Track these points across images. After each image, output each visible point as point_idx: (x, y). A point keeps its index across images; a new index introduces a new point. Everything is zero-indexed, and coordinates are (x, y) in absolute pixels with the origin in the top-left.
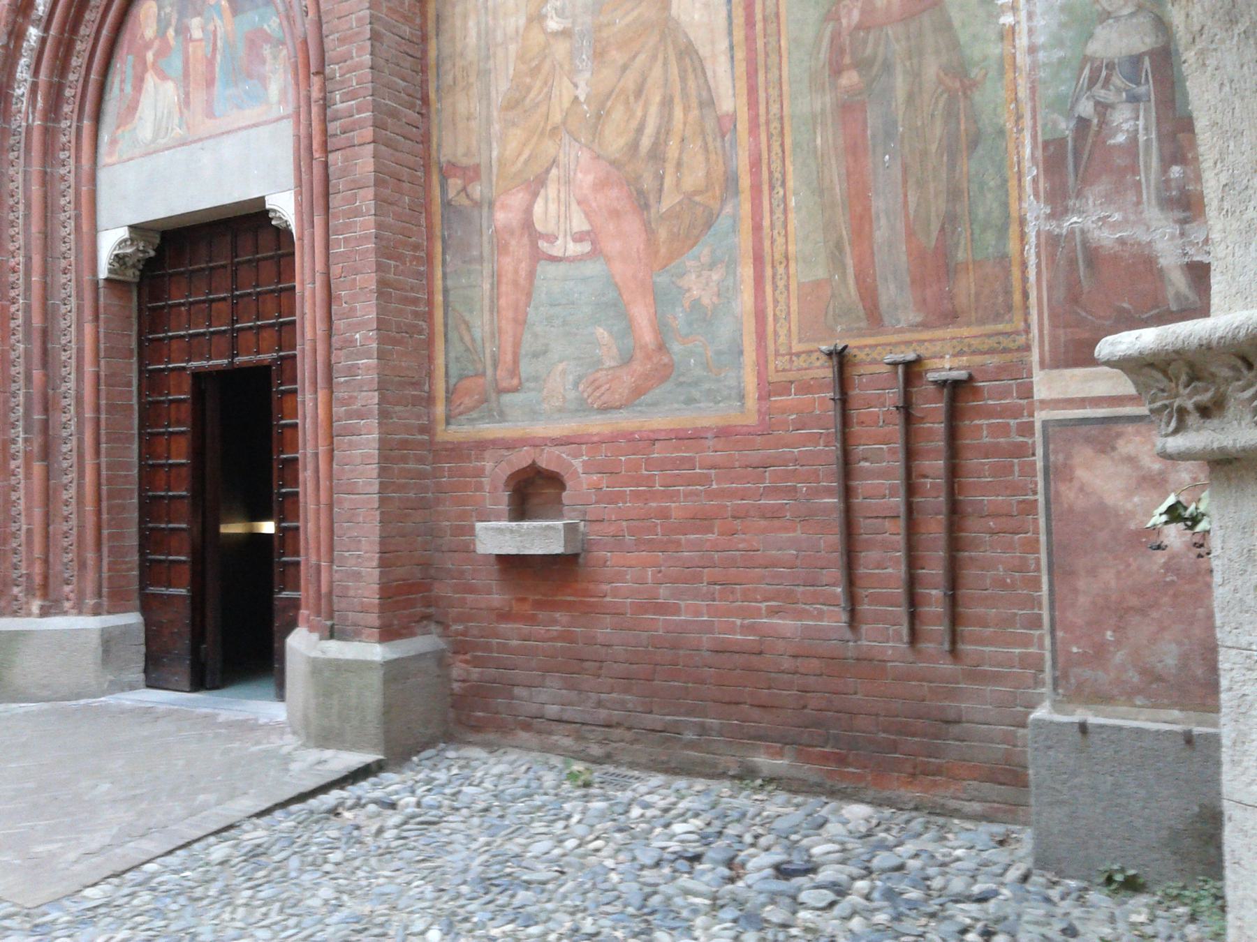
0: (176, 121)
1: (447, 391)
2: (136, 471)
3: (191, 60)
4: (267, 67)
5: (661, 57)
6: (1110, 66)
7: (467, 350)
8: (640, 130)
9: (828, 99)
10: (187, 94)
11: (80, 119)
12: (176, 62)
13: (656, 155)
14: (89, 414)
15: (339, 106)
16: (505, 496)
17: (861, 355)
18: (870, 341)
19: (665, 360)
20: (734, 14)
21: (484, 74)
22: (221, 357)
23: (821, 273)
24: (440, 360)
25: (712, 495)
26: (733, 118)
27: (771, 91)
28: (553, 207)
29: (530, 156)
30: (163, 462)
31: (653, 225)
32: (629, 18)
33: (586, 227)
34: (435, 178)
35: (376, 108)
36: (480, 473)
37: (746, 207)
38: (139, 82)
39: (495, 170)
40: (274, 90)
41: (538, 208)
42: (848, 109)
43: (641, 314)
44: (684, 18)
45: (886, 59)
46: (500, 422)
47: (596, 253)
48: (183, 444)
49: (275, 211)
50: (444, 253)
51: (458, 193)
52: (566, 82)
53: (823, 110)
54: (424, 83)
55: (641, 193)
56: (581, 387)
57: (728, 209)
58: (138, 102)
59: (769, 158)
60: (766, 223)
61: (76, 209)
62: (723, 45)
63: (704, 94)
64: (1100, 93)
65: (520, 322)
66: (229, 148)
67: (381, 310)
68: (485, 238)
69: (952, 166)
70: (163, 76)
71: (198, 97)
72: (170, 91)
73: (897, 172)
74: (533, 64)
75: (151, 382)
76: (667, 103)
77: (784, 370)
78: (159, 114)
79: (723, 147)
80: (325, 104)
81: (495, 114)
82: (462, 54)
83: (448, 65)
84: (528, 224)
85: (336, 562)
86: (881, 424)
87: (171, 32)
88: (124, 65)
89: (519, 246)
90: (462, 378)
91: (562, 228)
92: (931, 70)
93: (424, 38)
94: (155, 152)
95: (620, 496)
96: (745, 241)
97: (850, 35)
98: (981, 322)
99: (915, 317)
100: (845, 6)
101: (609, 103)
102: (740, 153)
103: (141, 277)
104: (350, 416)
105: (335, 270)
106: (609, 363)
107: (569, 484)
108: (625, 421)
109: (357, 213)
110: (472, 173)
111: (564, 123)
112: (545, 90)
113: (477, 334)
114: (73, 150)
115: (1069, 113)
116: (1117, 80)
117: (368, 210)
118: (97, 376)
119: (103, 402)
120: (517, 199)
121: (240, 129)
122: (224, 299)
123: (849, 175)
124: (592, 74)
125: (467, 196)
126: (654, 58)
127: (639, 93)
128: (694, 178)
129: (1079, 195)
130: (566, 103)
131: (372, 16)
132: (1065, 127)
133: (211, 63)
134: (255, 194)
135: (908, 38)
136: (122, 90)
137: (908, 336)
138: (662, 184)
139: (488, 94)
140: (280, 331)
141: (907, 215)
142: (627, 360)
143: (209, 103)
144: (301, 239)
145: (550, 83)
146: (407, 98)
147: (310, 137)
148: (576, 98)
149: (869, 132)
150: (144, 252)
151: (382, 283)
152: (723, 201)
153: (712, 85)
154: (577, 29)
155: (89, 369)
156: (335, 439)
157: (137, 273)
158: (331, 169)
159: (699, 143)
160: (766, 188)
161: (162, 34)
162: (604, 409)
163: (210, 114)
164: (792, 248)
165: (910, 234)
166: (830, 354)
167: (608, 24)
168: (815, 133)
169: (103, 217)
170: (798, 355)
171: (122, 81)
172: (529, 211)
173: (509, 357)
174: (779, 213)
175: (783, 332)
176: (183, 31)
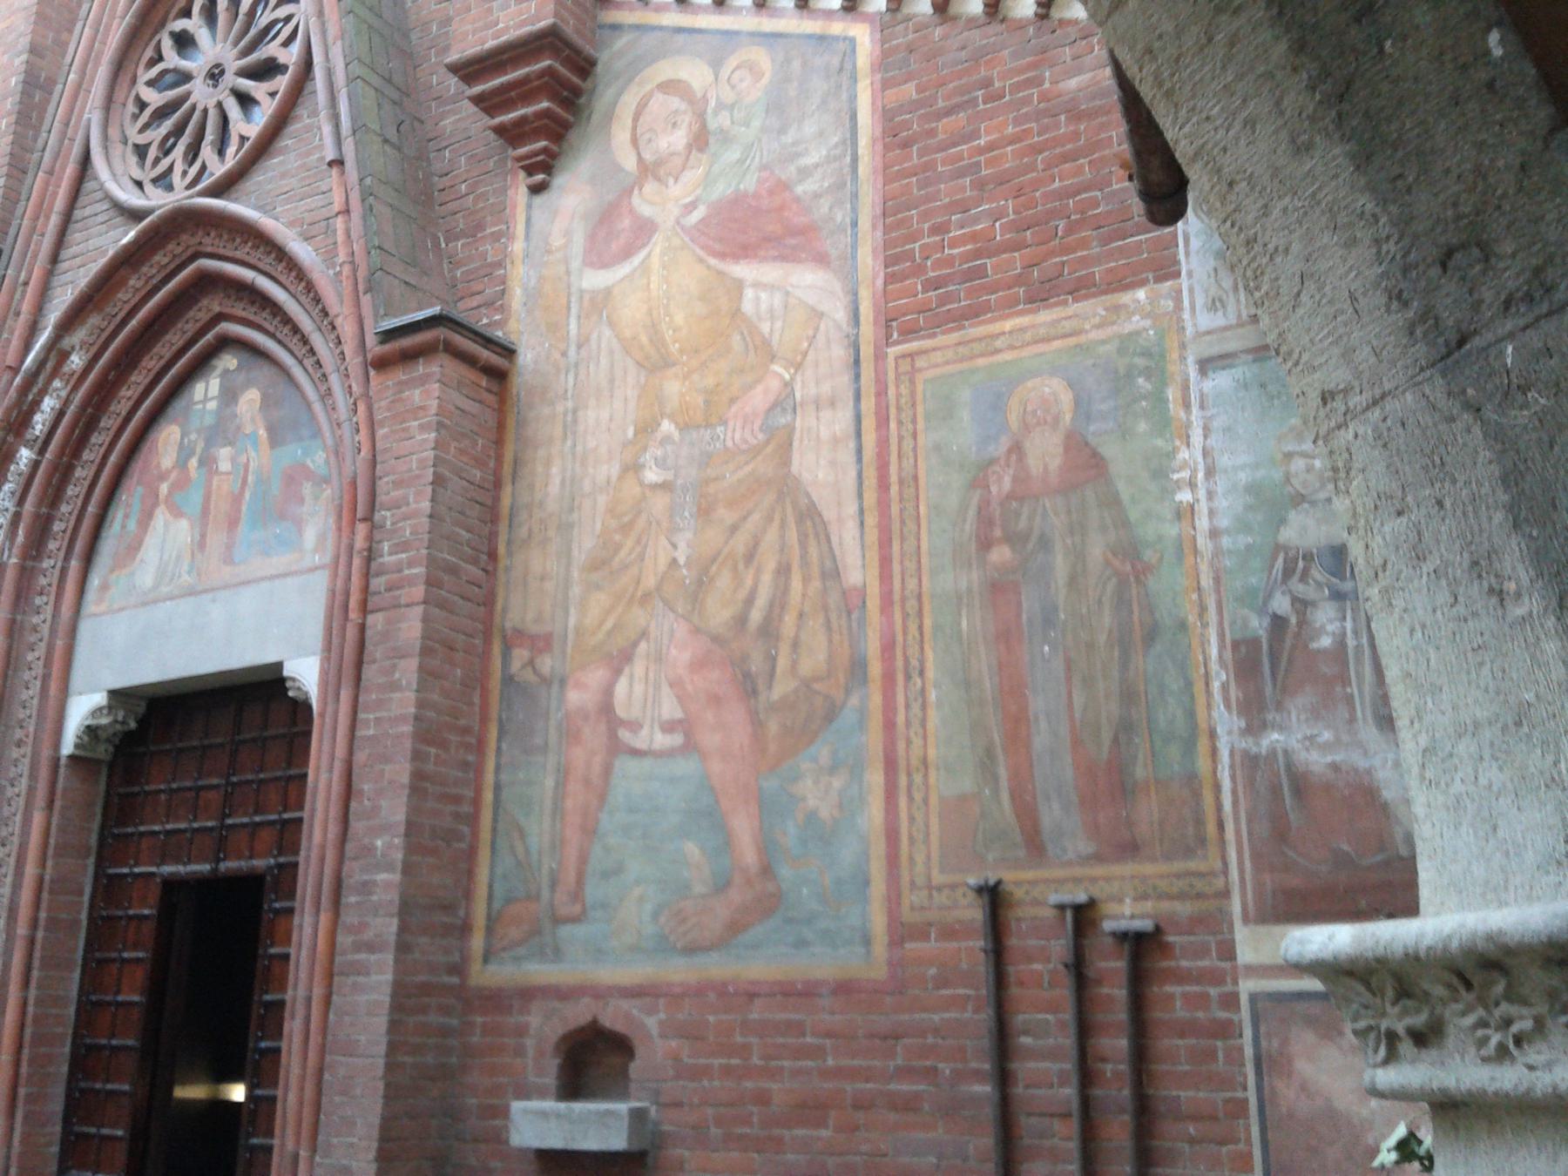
0: (186, 567)
1: (489, 917)
2: (72, 1010)
3: (213, 498)
4: (305, 509)
5: (777, 517)
6: (1308, 557)
7: (519, 863)
8: (750, 601)
9: (975, 575)
10: (203, 536)
11: (67, 559)
12: (195, 498)
13: (768, 631)
14: (22, 930)
15: (387, 559)
16: (553, 1065)
17: (1019, 893)
18: (1030, 875)
19: (771, 887)
20: (865, 474)
21: (566, 528)
22: (199, 860)
23: (967, 784)
24: (483, 874)
25: (825, 1074)
26: (862, 592)
27: (907, 563)
28: (639, 689)
29: (615, 627)
30: (109, 998)
31: (762, 716)
32: (741, 474)
33: (679, 715)
34: (497, 649)
35: (431, 561)
36: (521, 1031)
37: (876, 700)
39: (570, 644)
40: (310, 535)
41: (621, 688)
42: (999, 590)
43: (743, 827)
44: (806, 477)
45: (1042, 537)
46: (553, 961)
47: (690, 746)
48: (139, 975)
49: (293, 679)
50: (499, 740)
51: (524, 667)
52: (663, 541)
53: (969, 590)
54: (493, 536)
55: (747, 675)
56: (663, 919)
57: (854, 701)
58: (140, 543)
59: (905, 640)
60: (901, 719)
61: (45, 666)
62: (851, 508)
63: (828, 564)
64: (1299, 588)
65: (590, 831)
66: (248, 601)
67: (414, 811)
68: (553, 723)
69: (1125, 664)
70: (177, 512)
71: (216, 540)
73: (1058, 665)
74: (626, 519)
75: (108, 889)
76: (783, 571)
77: (922, 908)
78: (166, 557)
79: (850, 628)
80: (370, 556)
81: (575, 574)
82: (541, 504)
83: (523, 515)
84: (606, 708)
85: (319, 1151)
86: (1046, 985)
87: (194, 462)
88: (131, 496)
89: (593, 736)
90: (509, 901)
91: (649, 713)
92: (1096, 550)
93: (498, 484)
94: (155, 601)
95: (705, 1071)
96: (874, 739)
97: (1002, 504)
98: (1168, 857)
99: (1085, 847)
100: (994, 473)
101: (714, 568)
102: (870, 634)
103: (115, 755)
104: (359, 947)
105: (360, 757)
106: (699, 889)
107: (640, 1051)
108: (716, 967)
109: (394, 686)
110: (542, 643)
111: (658, 588)
112: (638, 549)
113: (534, 842)
114: (52, 598)
115: (1262, 610)
116: (1317, 573)
117: (409, 683)
118: (40, 880)
119: (43, 915)
120: (595, 677)
121: (263, 579)
122: (216, 787)
123: (1000, 666)
124: (695, 534)
125: (534, 668)
126: (769, 519)
127: (750, 557)
128: (814, 659)
129: (1279, 706)
130: (662, 567)
131: (436, 457)
132: (1258, 625)
133: (237, 499)
134: (270, 658)
135: (1069, 512)
136: (123, 527)
137: (1078, 871)
138: (773, 669)
139: (569, 550)
140: (282, 832)
141: (1072, 718)
142: (722, 886)
143: (229, 547)
144: (322, 715)
145: (644, 540)
146: (470, 551)
147: (347, 594)
148: (674, 561)
149: (1024, 617)
150: (123, 723)
151: (418, 776)
152: (848, 692)
153: (837, 553)
154: (679, 482)
155: (30, 870)
156: (336, 979)
157: (111, 749)
158: (369, 633)
159: (821, 620)
160: (900, 677)
161: (182, 464)
162: (691, 950)
163: (228, 559)
164: (932, 753)
165: (1076, 743)
166: (980, 890)
167: (716, 479)
168: (960, 615)
169: (78, 676)
170: (939, 889)
171: (126, 516)
172: (608, 692)
173: (570, 876)
174: (916, 708)
175: (920, 859)
176: (208, 462)
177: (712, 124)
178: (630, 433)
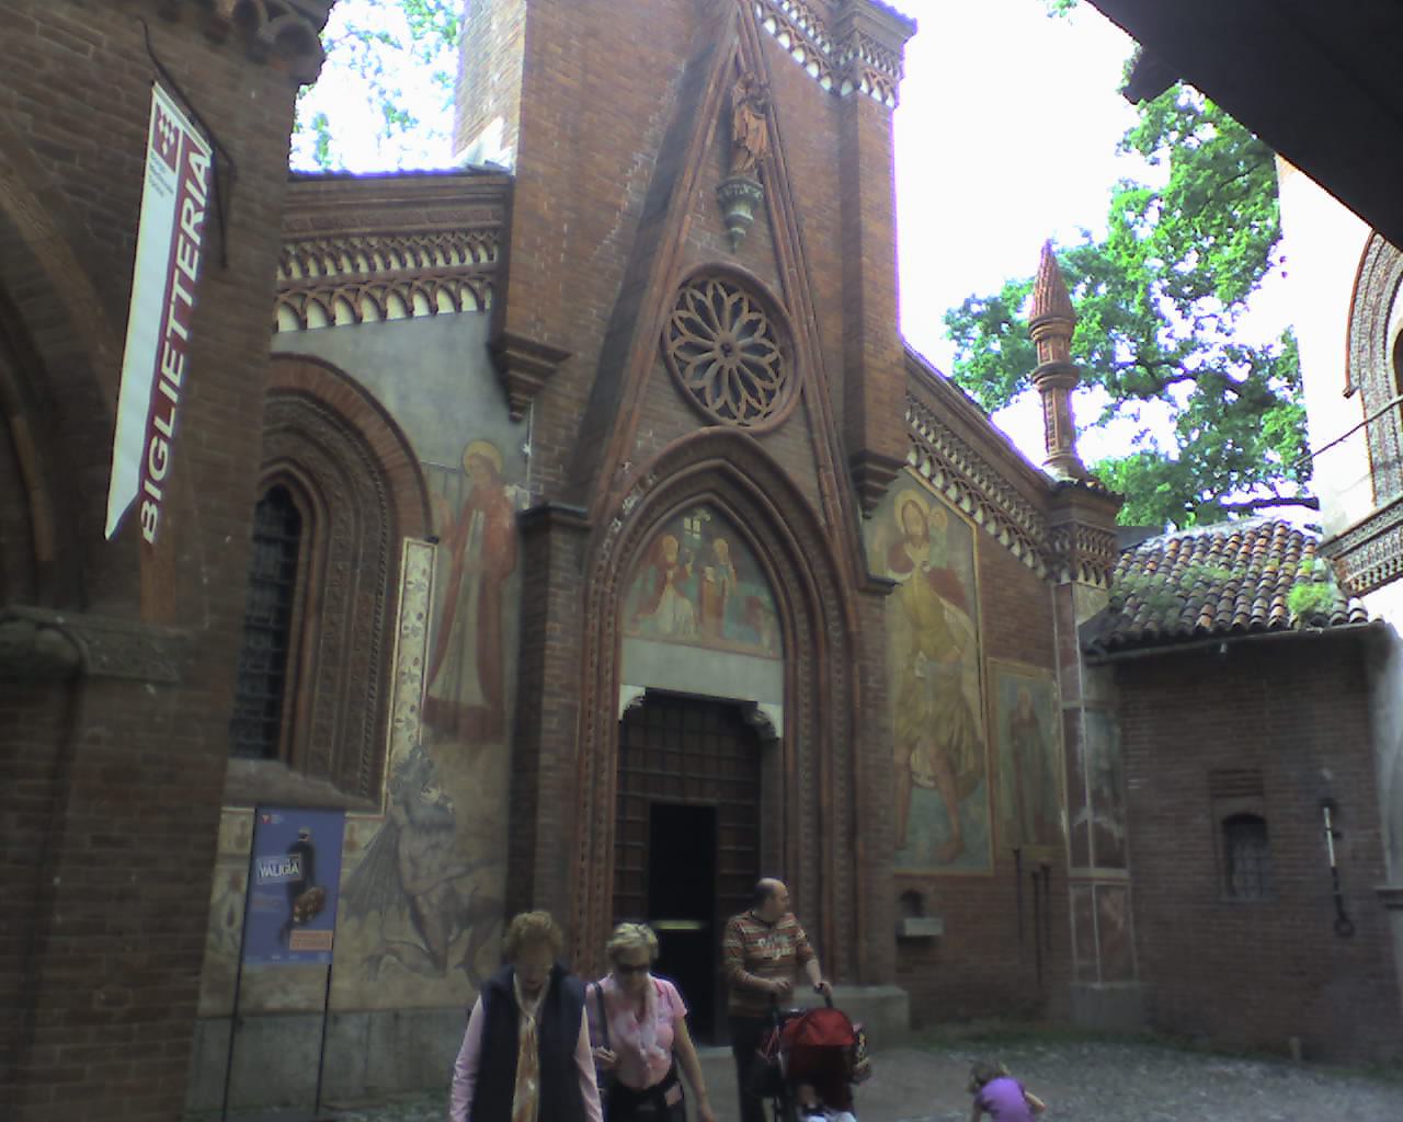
0: (692, 628)
10: (701, 614)
12: (693, 590)
13: (958, 750)
38: (660, 588)
40: (766, 640)
66: (734, 663)
70: (682, 593)
72: (687, 607)
84: (908, 765)
87: (689, 567)
128: (971, 766)
133: (720, 601)
134: (751, 698)
169: (626, 670)
172: (909, 758)
176: (699, 571)
177: (932, 532)
178: (910, 651)
